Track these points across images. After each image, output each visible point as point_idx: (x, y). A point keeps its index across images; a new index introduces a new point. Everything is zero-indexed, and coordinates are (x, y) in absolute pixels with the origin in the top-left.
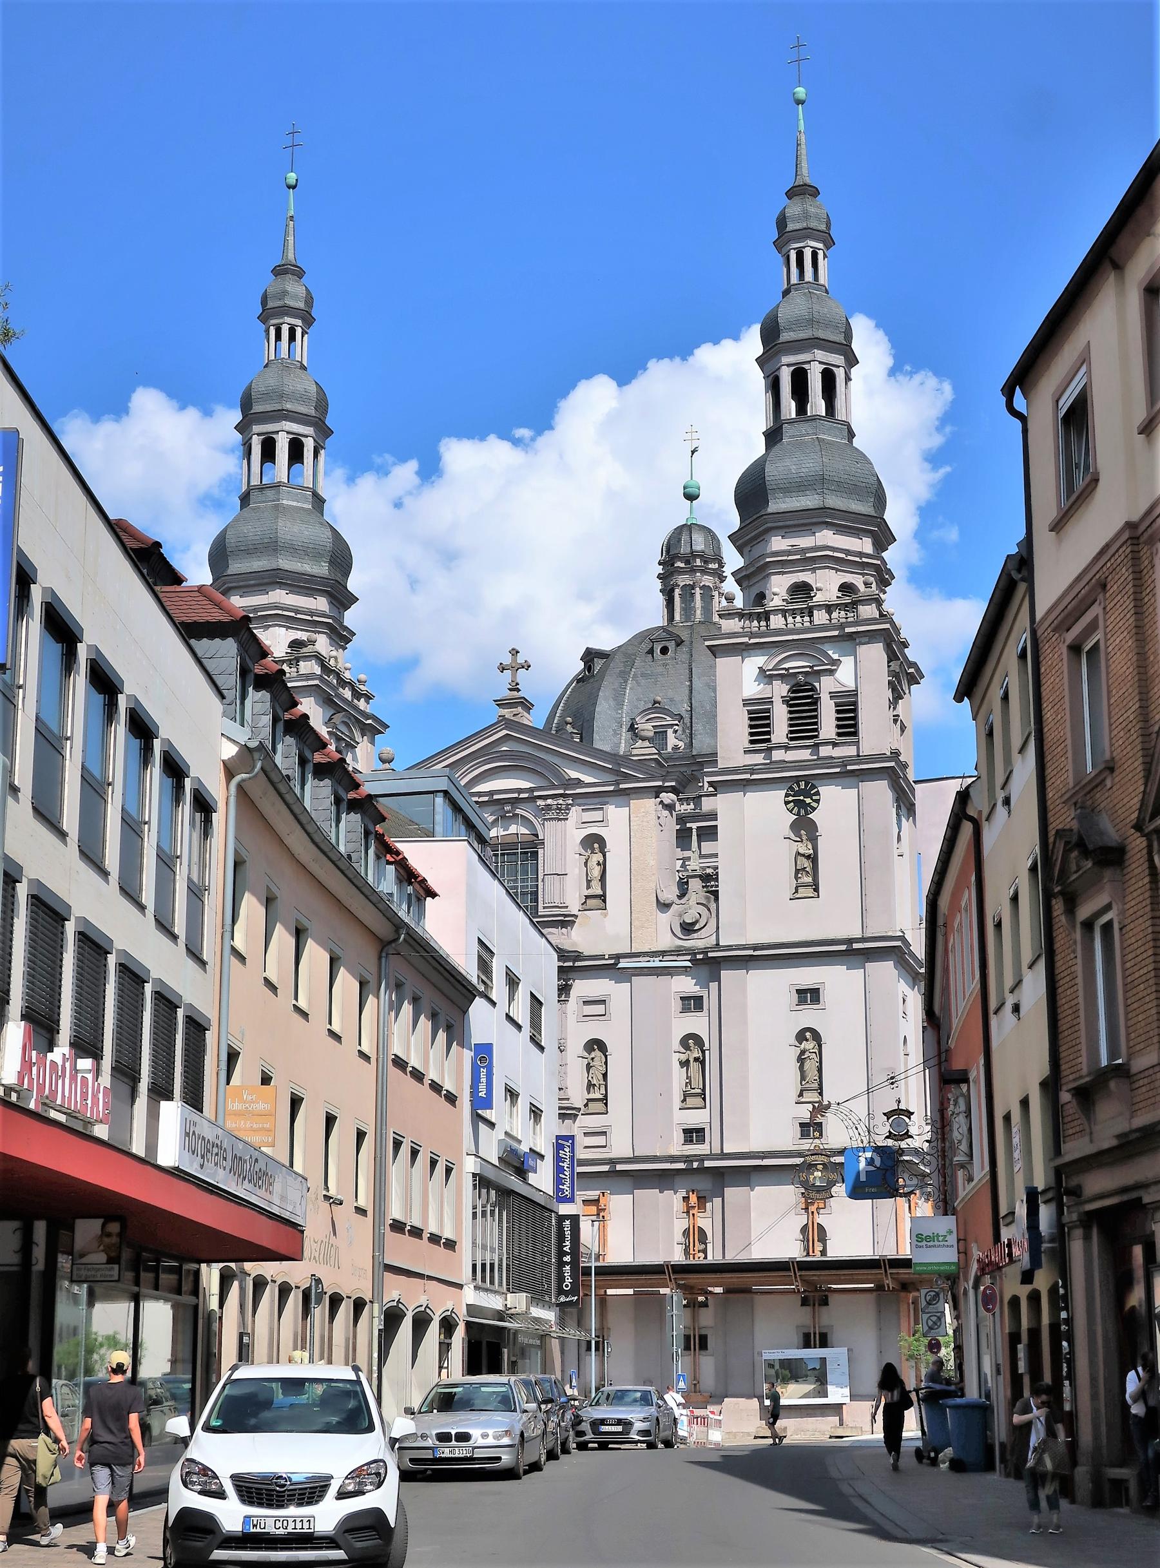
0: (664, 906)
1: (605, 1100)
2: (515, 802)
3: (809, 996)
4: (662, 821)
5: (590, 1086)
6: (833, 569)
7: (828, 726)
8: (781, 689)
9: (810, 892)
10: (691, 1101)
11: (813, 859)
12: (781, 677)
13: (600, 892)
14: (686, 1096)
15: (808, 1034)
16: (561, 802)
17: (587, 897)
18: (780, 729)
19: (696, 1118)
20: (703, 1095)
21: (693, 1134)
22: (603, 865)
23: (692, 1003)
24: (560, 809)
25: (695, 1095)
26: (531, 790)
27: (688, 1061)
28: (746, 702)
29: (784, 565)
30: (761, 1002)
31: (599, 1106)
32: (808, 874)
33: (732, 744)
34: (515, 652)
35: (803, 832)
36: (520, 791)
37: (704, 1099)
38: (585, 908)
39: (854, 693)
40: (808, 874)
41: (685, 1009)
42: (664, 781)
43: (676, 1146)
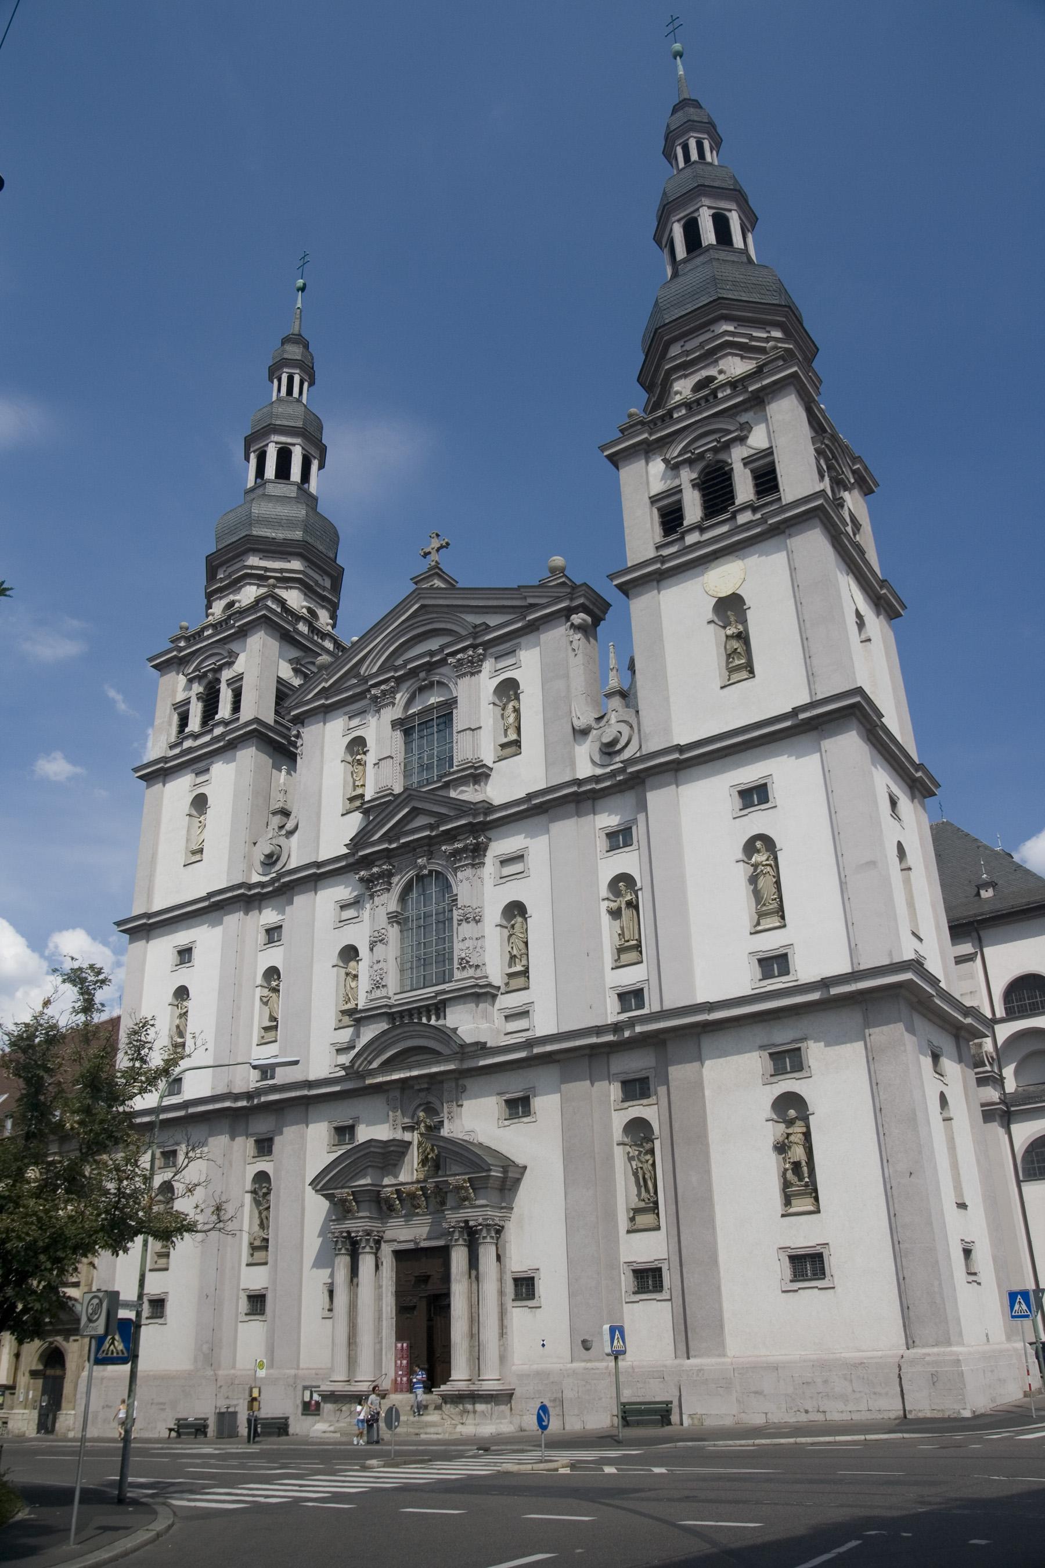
0: (582, 733)
1: (525, 973)
2: (430, 667)
3: (755, 796)
4: (575, 645)
6: (737, 355)
7: (744, 489)
8: (687, 476)
10: (626, 958)
11: (743, 637)
12: (690, 462)
14: (621, 950)
15: (759, 844)
16: (471, 653)
19: (631, 976)
20: (638, 947)
21: (630, 997)
22: (517, 711)
23: (619, 838)
24: (470, 661)
25: (629, 949)
26: (442, 648)
27: (619, 909)
28: (654, 500)
29: (685, 368)
30: (701, 816)
31: (520, 982)
32: (740, 659)
33: (642, 538)
35: (729, 613)
36: (432, 654)
37: (641, 952)
39: (769, 452)
41: (613, 847)
42: (572, 599)
43: (611, 1012)
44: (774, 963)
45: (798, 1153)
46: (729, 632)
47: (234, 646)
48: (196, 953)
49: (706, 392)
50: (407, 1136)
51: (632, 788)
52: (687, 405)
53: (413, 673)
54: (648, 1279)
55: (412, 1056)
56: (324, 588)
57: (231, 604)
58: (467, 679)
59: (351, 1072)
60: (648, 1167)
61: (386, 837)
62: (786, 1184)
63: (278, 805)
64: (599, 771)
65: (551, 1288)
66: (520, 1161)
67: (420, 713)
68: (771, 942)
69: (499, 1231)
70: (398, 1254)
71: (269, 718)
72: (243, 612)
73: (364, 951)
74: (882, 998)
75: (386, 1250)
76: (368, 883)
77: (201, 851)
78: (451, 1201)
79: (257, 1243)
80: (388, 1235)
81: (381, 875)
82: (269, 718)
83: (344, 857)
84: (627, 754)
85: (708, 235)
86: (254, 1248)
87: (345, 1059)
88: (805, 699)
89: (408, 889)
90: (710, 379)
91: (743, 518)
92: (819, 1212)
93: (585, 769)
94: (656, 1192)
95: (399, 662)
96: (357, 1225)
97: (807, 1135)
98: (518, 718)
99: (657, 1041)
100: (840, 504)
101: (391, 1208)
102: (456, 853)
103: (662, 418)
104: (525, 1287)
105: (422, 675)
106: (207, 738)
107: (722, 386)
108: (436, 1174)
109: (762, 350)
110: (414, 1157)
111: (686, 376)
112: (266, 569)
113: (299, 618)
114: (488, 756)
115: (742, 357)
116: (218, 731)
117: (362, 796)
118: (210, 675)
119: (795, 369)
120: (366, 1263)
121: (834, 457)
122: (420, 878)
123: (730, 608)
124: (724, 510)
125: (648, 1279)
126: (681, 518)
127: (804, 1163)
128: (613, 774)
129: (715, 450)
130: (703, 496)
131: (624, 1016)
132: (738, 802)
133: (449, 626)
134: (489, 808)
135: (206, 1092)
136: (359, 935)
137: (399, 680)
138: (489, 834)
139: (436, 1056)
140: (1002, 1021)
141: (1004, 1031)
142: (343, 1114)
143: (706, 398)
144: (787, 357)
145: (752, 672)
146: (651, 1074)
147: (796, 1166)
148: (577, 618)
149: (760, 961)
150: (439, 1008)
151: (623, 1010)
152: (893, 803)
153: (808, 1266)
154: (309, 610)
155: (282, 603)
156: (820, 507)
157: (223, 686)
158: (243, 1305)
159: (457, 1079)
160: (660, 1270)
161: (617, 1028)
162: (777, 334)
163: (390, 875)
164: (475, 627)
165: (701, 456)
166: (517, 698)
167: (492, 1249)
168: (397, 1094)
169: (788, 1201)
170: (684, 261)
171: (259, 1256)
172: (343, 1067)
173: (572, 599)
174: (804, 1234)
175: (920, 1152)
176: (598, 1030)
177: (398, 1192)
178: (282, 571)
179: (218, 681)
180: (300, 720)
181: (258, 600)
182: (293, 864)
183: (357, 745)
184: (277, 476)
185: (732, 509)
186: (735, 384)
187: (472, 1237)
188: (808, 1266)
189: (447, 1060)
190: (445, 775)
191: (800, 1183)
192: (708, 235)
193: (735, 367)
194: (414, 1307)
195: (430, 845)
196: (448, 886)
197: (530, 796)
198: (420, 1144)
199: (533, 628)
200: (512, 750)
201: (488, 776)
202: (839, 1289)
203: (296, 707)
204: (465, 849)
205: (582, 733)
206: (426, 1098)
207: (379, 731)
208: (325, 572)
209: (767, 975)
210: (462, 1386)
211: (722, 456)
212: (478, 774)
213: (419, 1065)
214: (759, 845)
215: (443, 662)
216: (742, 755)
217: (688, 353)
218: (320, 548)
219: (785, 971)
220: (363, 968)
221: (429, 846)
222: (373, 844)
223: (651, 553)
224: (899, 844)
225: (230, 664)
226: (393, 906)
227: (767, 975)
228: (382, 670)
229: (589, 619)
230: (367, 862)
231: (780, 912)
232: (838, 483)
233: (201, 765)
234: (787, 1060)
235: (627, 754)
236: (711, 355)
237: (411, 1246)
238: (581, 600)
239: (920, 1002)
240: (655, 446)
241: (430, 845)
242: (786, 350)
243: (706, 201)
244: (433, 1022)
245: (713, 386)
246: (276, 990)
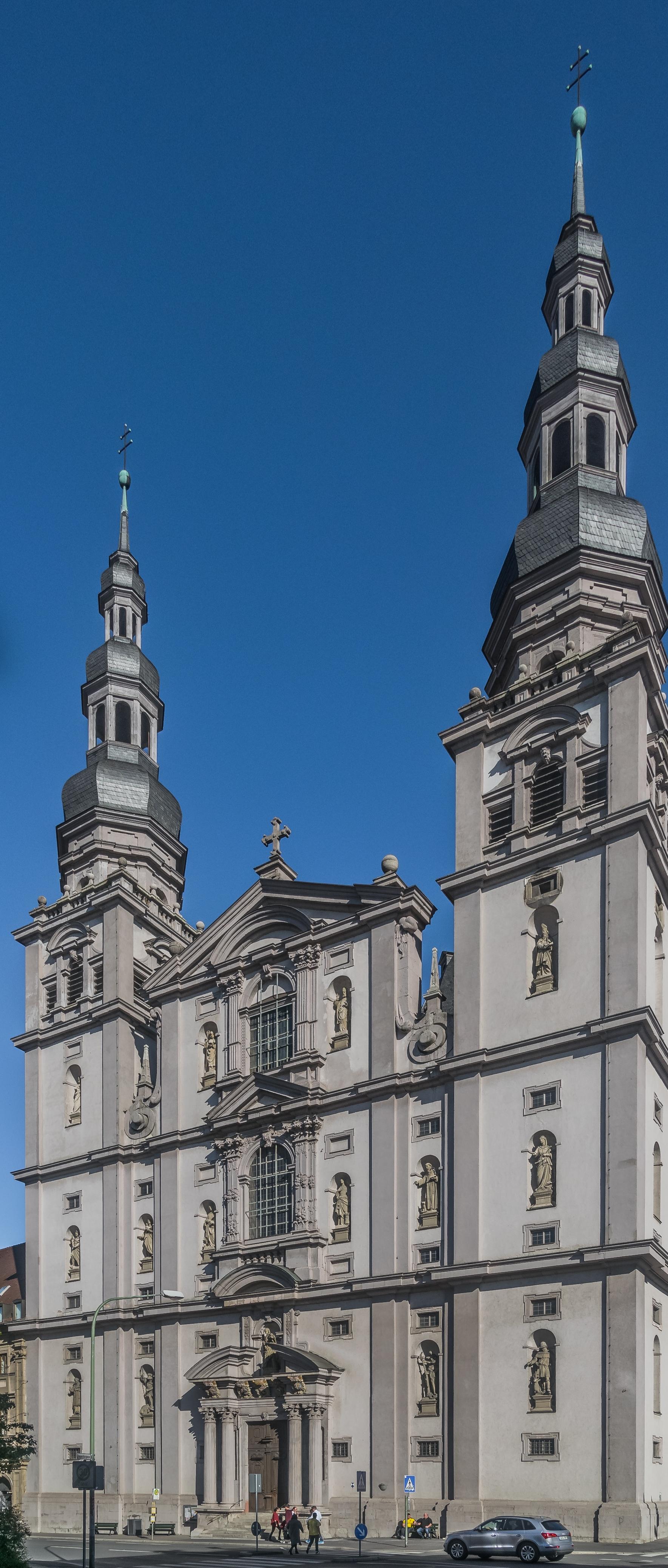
15: (543, 1139)
32: (547, 969)
33: (472, 840)
40: (547, 969)
44: (544, 1235)
45: (545, 1370)
62: (532, 1392)
68: (543, 1217)
126: (510, 821)
127: (548, 1378)
132: (530, 1101)
147: (543, 1380)
169: (533, 1403)
174: (543, 1425)
190: (286, 1063)
191: (543, 1390)
203: (155, 989)
209: (537, 1242)
219: (551, 1239)
227: (537, 1242)
240: (494, 737)
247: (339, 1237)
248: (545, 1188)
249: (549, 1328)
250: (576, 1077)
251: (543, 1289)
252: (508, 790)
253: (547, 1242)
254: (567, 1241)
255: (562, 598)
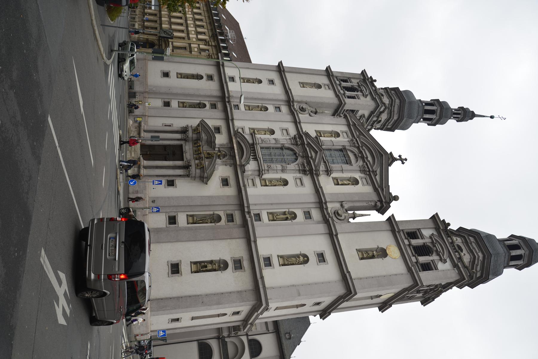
3: (321, 257)
4: (370, 203)
5: (271, 181)
7: (423, 259)
8: (427, 241)
9: (361, 256)
11: (373, 257)
12: (432, 242)
13: (340, 183)
15: (306, 259)
17: (337, 180)
18: (414, 242)
19: (264, 216)
20: (274, 220)
21: (258, 217)
22: (348, 184)
23: (308, 215)
26: (369, 161)
28: (419, 230)
29: (466, 243)
31: (263, 183)
34: (406, 160)
36: (367, 158)
38: (334, 179)
39: (436, 269)
42: (385, 202)
46: (374, 252)
47: (369, 98)
48: (272, 86)
49: (457, 249)
50: (217, 149)
51: (324, 220)
52: (452, 243)
53: (361, 152)
54: (172, 220)
55: (242, 150)
56: (388, 125)
57: (383, 95)
58: (359, 169)
59: (237, 133)
60: (206, 221)
61: (309, 144)
62: (200, 262)
63: (318, 111)
64: (329, 210)
65: (170, 192)
66: (209, 183)
67: (348, 155)
68: (275, 261)
69: (188, 176)
70: (181, 146)
71: (346, 108)
72: (380, 99)
73: (273, 136)
74: (258, 295)
75: (182, 142)
76: (295, 138)
77: (304, 87)
78: (197, 161)
79: (185, 104)
80: (187, 143)
81: (297, 142)
82: (346, 108)
83: (302, 131)
84: (335, 218)
85: (514, 253)
86: (183, 103)
87: (240, 130)
88: (353, 276)
89: (292, 150)
90: (462, 251)
91: (414, 259)
92: (192, 272)
93: (330, 206)
94: (199, 223)
95: (364, 148)
96: (190, 134)
97: (215, 270)
98: (346, 185)
99: (245, 224)
100: (418, 292)
101: (195, 144)
102: (303, 164)
103: (447, 234)
104: (171, 183)
105: (360, 155)
106: (339, 88)
107: (460, 254)
108: (205, 158)
109: (473, 268)
110: (211, 151)
111: (463, 242)
112: (394, 106)
113: (378, 117)
114: (334, 175)
115: (470, 262)
116: (342, 92)
117: (321, 136)
118: (360, 89)
119: (467, 279)
120: (178, 136)
121: (435, 291)
122: (295, 154)
123: (383, 253)
124: (416, 253)
125: (172, 220)
126: (413, 239)
128: (328, 214)
129: (437, 251)
130: (421, 246)
131: (252, 215)
133: (376, 163)
134: (318, 175)
135: (230, 88)
136: (278, 135)
137: (358, 148)
138: (309, 175)
139: (241, 157)
140: (248, 338)
141: (244, 339)
142: (224, 129)
143: (455, 249)
144: (471, 277)
145: (362, 259)
146: (234, 223)
147: (206, 267)
148: (379, 204)
149: (269, 258)
150: (256, 159)
151: (254, 214)
152: (318, 304)
153: (175, 269)
154: (380, 121)
155: (383, 112)
156: (418, 285)
157: (356, 93)
158: (167, 100)
159: (234, 164)
160: (175, 224)
161: (249, 213)
162: (479, 275)
163: (297, 145)
164: (376, 171)
165: (435, 246)
166: (353, 184)
167: (182, 174)
168: (229, 146)
169: (195, 263)
170: (504, 244)
171: (181, 105)
172: (237, 130)
173: (385, 202)
174: (185, 268)
175: (209, 305)
176: (248, 207)
177: (200, 146)
178: (394, 111)
179: (358, 92)
180: (345, 117)
181: (384, 104)
182: (300, 115)
183: (337, 135)
184: (425, 110)
185: (416, 255)
186: (460, 259)
187: (187, 167)
188: (175, 269)
189: (240, 161)
191: (201, 267)
192: (514, 253)
193: (467, 258)
194: (165, 150)
195: (306, 157)
196: (293, 163)
197: (321, 188)
198: (215, 153)
199: (376, 190)
200: (336, 183)
201: (328, 175)
202: (168, 278)
204: (305, 167)
205: (342, 205)
206: (228, 154)
207: (343, 140)
208: (393, 125)
210: (142, 164)
211: (434, 254)
212: (328, 172)
213: (238, 153)
214: (304, 259)
215: (364, 161)
216: (334, 255)
217: (471, 243)
218: (401, 124)
219: (266, 265)
220: (268, 136)
221: (306, 156)
222: (306, 139)
223: (401, 228)
224: (305, 305)
225: (363, 95)
226: (287, 145)
228: (362, 142)
229: (378, 208)
230: (301, 137)
231: (284, 265)
232: (426, 292)
233: (331, 87)
234: (238, 264)
235: (335, 218)
236: (471, 251)
237: (184, 150)
238: (385, 205)
239: (255, 308)
241: (306, 157)
242: (473, 276)
243: (527, 253)
244: (251, 157)
245: (459, 251)
246: (261, 110)
247: (263, 182)
248: (288, 261)
249: (229, 268)
250: (329, 272)
251: (246, 264)
252: (422, 237)
253: (265, 264)
254: (267, 273)
255: (478, 251)
